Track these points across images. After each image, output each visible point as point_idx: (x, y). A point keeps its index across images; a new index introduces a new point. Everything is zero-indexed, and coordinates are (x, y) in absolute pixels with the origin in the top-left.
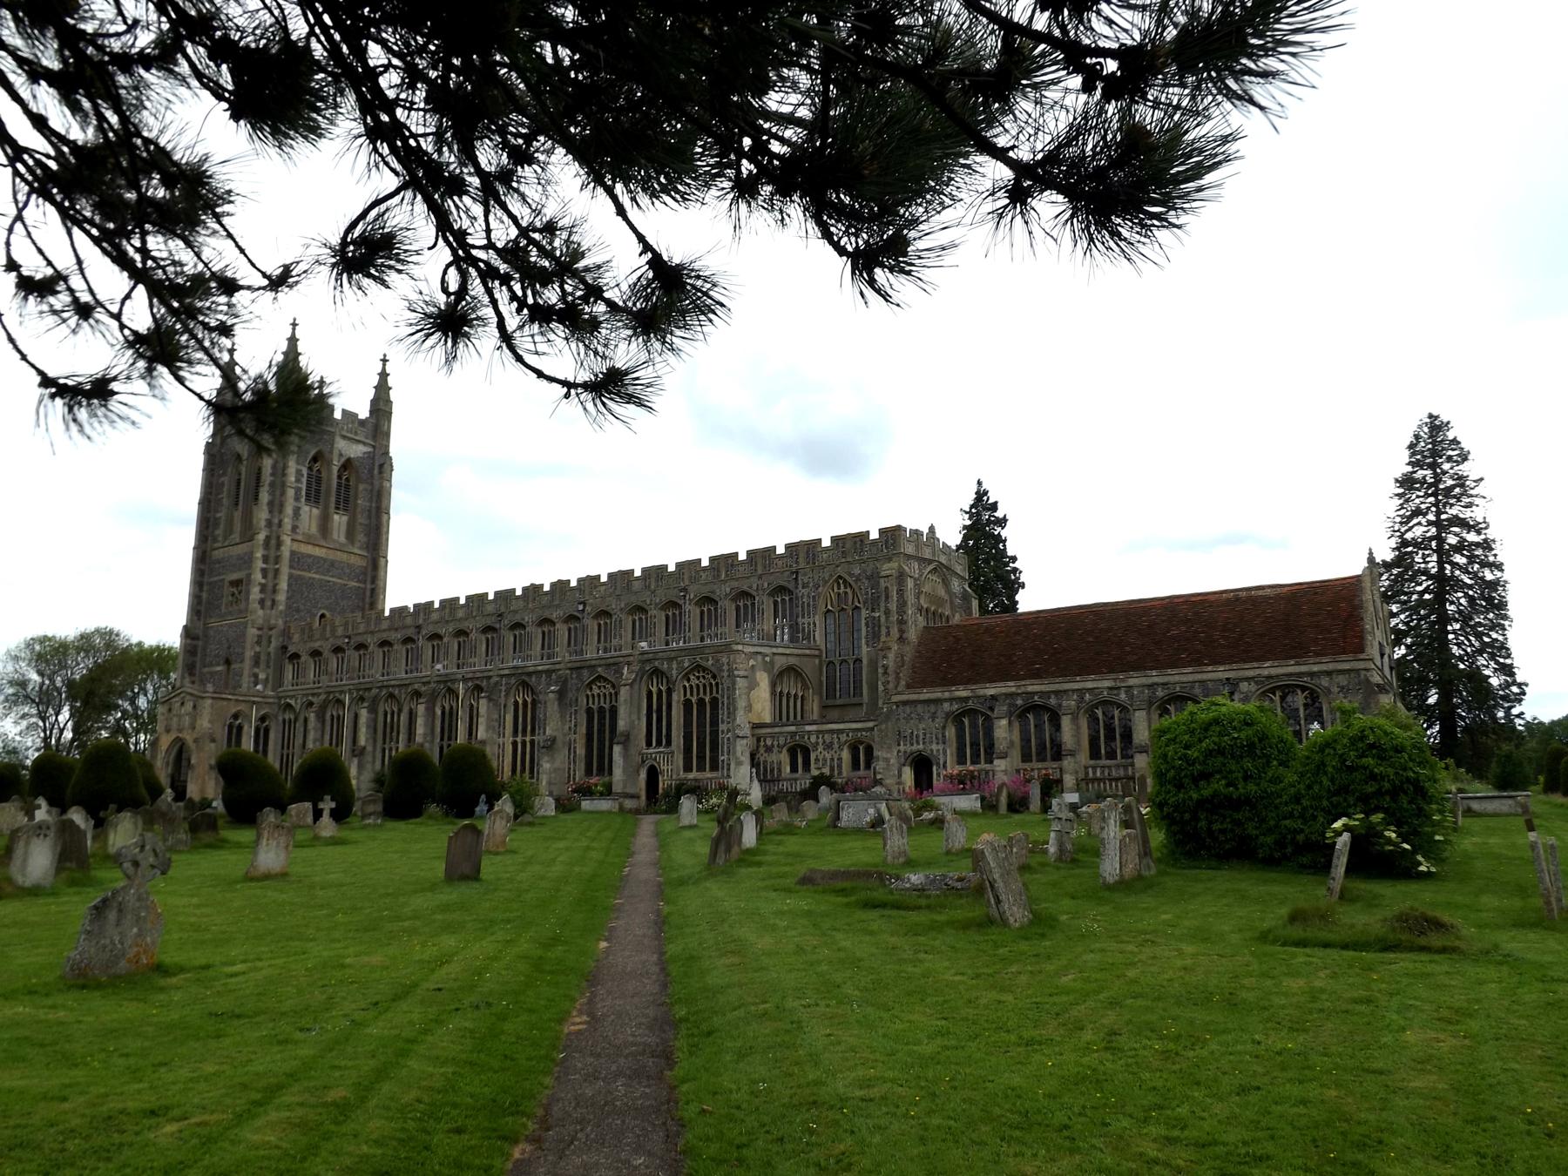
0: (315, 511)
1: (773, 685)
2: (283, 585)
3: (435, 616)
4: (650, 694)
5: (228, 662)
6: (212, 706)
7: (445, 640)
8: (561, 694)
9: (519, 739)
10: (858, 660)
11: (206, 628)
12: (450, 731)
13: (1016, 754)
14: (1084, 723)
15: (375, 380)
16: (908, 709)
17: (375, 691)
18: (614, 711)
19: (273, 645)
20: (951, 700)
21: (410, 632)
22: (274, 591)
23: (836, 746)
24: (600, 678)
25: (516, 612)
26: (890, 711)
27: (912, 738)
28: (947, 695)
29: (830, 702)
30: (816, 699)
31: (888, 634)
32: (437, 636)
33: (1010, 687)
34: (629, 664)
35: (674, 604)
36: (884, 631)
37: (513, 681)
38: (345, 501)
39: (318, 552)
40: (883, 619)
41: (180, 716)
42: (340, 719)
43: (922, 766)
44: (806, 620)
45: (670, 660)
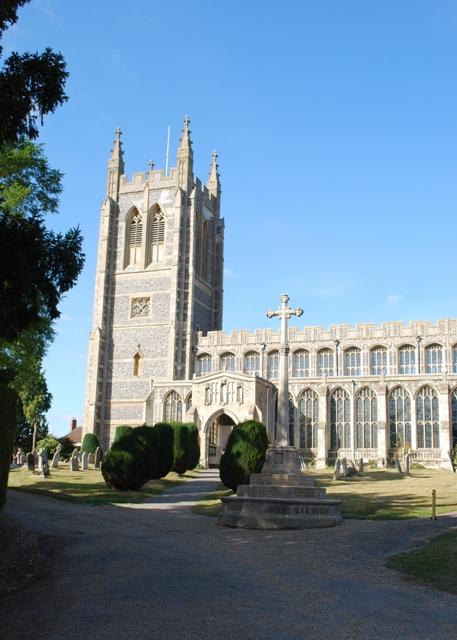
5: (137, 357)
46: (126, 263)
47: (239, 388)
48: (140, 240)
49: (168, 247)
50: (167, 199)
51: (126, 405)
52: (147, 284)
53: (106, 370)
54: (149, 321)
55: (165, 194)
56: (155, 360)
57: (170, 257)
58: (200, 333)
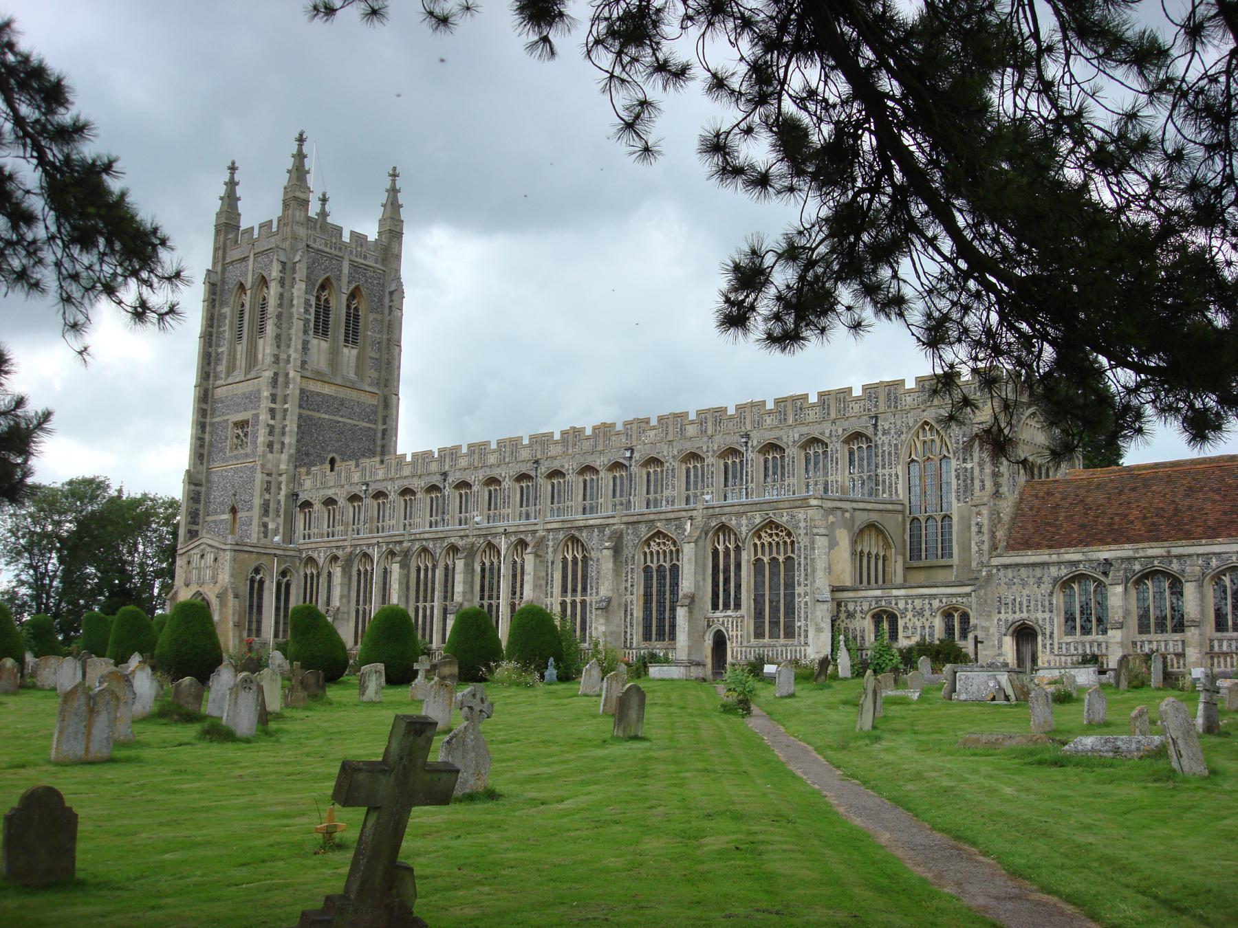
0: (324, 345)
1: (854, 543)
2: (292, 425)
3: (463, 463)
4: (715, 553)
5: (234, 511)
6: (234, 559)
7: (475, 488)
8: (617, 550)
9: (568, 600)
10: (947, 517)
12: (491, 589)
13: (1133, 622)
14: (1209, 590)
16: (1010, 573)
17: (405, 544)
18: (675, 569)
19: (283, 493)
20: (1059, 563)
21: (436, 479)
22: (283, 434)
23: (927, 613)
24: (659, 534)
25: (555, 458)
26: (990, 575)
27: (1014, 605)
28: (1054, 558)
29: (915, 564)
30: (900, 559)
31: (983, 487)
32: (465, 484)
33: (1126, 551)
34: (691, 518)
35: (733, 452)
36: (977, 483)
37: (561, 536)
38: (352, 333)
39: (327, 390)
40: (977, 472)
41: (199, 569)
42: (366, 577)
43: (1025, 634)
44: (886, 471)
45: (739, 515)
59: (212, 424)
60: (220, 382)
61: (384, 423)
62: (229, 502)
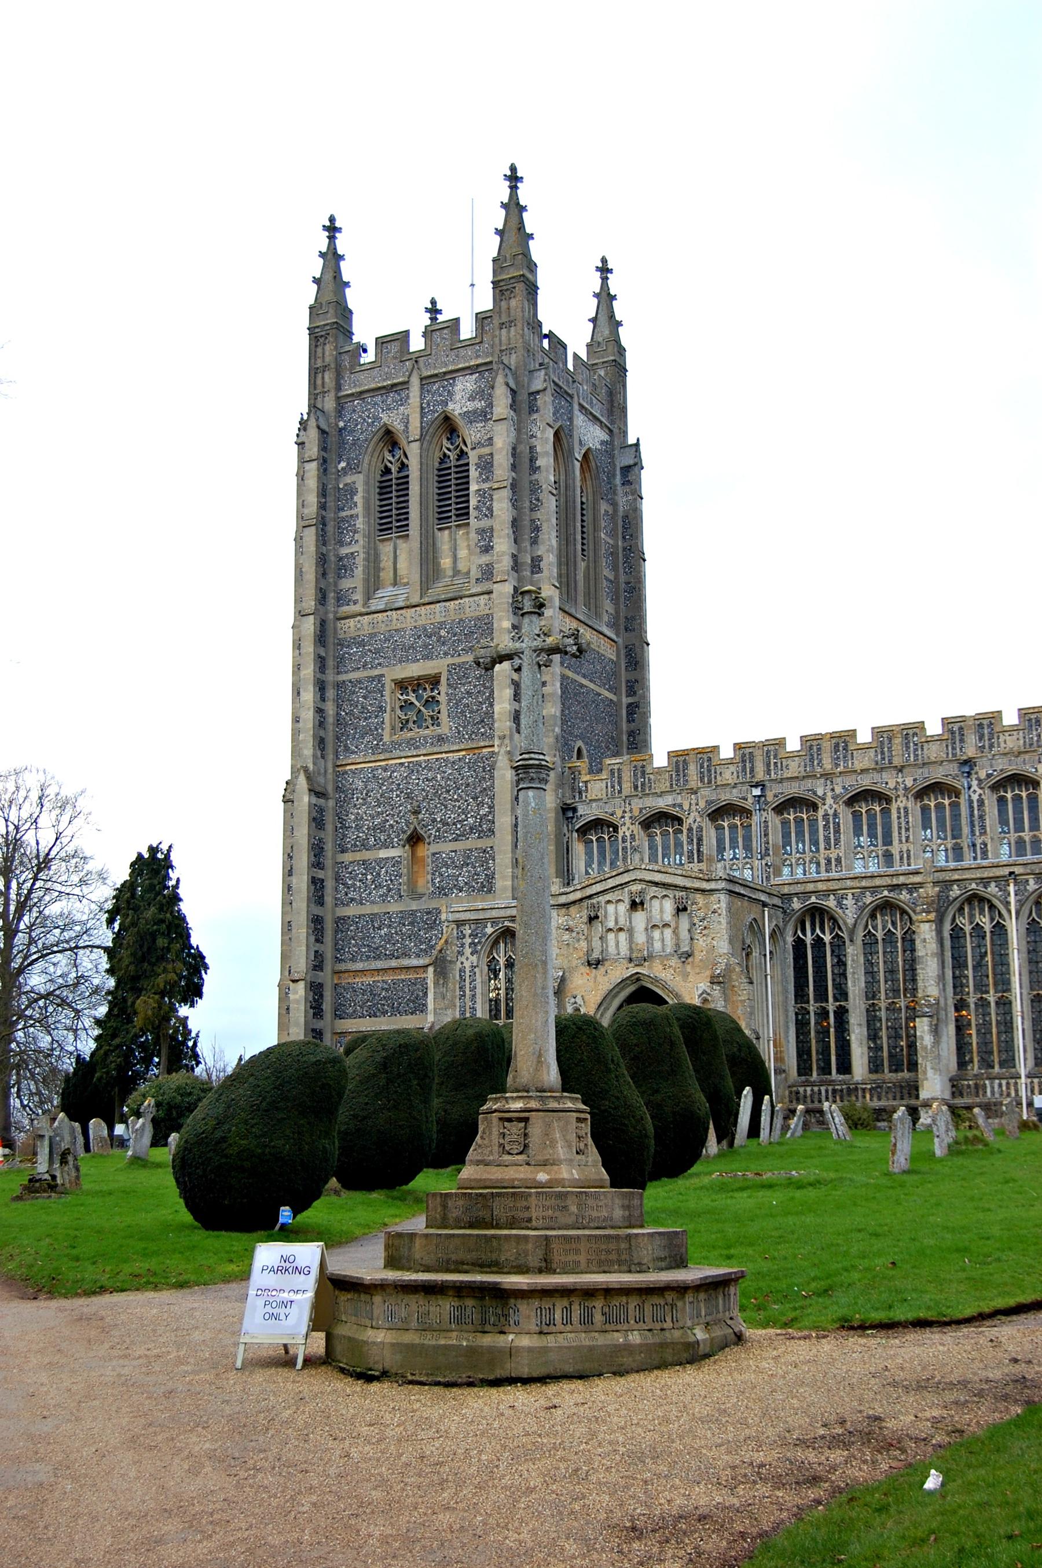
5: (415, 839)
11: (340, 774)
15: (591, 307)
46: (372, 585)
47: (681, 910)
48: (404, 516)
49: (481, 532)
50: (472, 398)
51: (389, 978)
52: (429, 641)
53: (329, 884)
54: (441, 739)
55: (465, 385)
56: (460, 846)
57: (485, 559)
58: (583, 765)
59: (339, 685)
60: (346, 609)
61: (631, 691)
62: (405, 824)
